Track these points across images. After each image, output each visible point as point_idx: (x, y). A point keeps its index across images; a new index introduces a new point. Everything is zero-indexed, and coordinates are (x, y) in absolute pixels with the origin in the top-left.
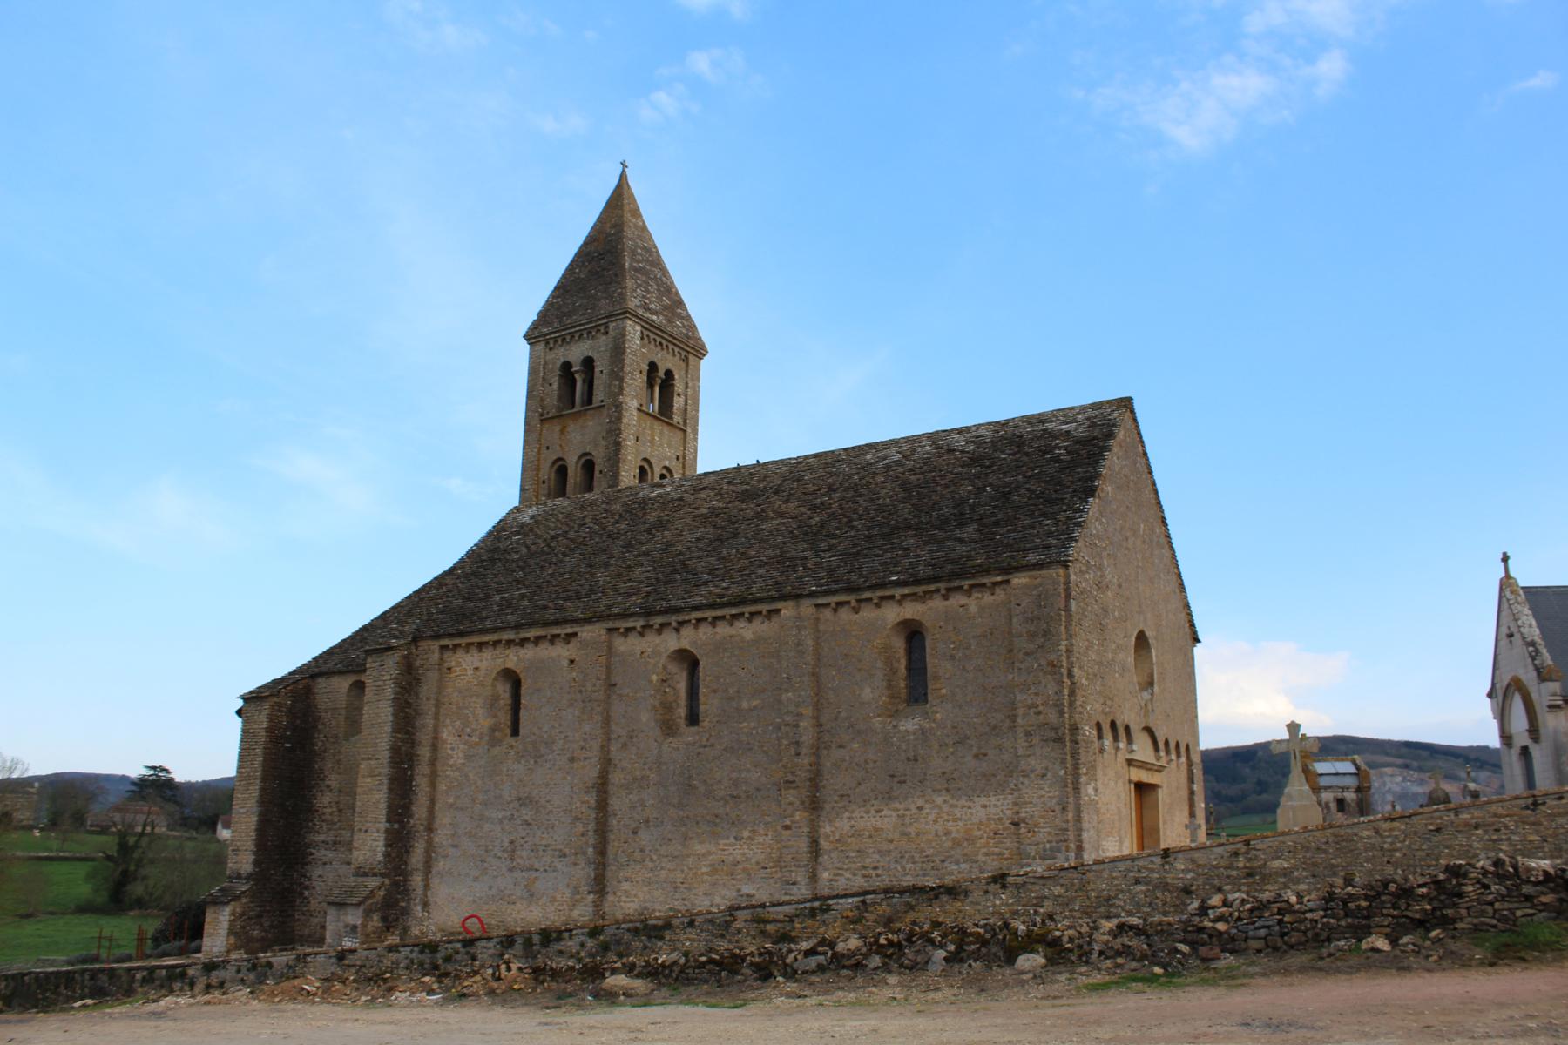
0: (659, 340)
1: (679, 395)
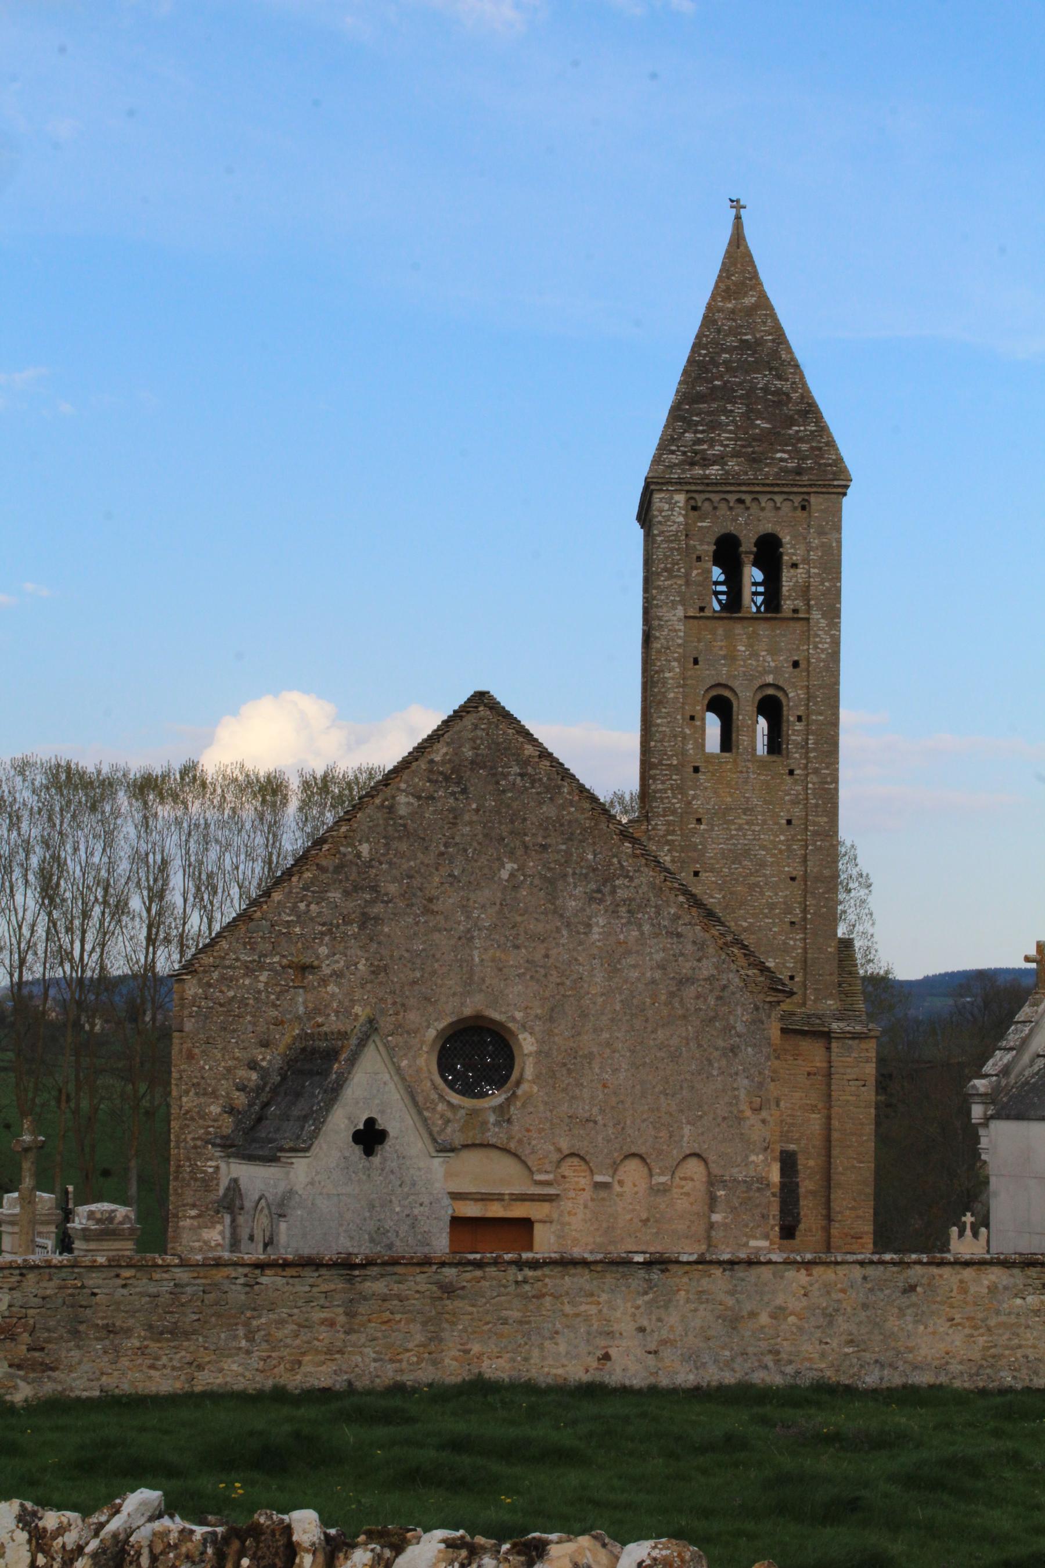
1: (795, 566)
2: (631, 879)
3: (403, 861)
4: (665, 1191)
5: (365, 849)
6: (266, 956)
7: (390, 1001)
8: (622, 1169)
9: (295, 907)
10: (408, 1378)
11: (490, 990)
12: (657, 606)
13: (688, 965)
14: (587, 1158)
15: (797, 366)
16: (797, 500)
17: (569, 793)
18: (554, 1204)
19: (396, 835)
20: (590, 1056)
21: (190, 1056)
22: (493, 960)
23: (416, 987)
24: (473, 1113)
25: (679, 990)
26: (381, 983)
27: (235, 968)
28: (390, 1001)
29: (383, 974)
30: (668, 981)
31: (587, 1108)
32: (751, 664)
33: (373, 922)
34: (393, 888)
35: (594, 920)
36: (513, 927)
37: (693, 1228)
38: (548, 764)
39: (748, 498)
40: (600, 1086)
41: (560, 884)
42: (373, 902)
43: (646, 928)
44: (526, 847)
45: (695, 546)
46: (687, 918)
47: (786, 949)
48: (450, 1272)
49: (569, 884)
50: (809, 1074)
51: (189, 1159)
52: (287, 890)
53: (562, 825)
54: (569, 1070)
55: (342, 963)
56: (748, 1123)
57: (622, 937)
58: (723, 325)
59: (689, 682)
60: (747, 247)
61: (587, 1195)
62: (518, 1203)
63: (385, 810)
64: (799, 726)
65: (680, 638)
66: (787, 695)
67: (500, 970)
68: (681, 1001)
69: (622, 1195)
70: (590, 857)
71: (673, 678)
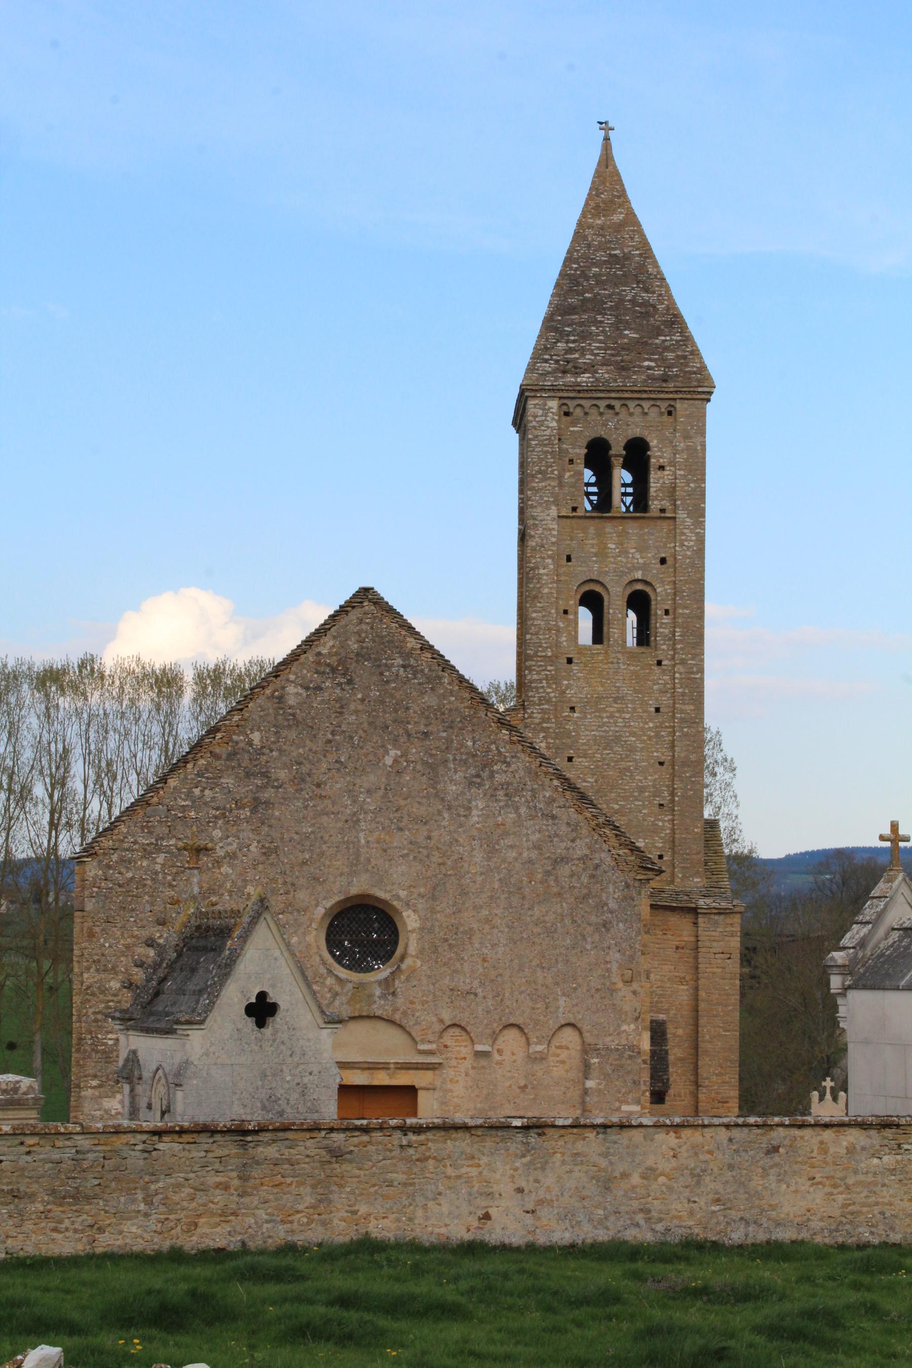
0: (602, 404)
1: (662, 468)
2: (508, 765)
3: (293, 748)
4: (542, 1059)
5: (256, 737)
6: (162, 839)
7: (280, 881)
8: (501, 1039)
9: (189, 794)
10: (299, 1239)
11: (375, 870)
12: (532, 507)
13: (563, 845)
14: (468, 1029)
15: (663, 279)
16: (664, 405)
17: (450, 684)
18: (437, 1072)
19: (286, 724)
20: (470, 933)
21: (91, 935)
22: (378, 842)
23: (305, 868)
24: (359, 987)
25: (554, 869)
26: (272, 864)
27: (133, 851)
28: (280, 881)
29: (274, 856)
30: (544, 861)
31: (468, 981)
32: (621, 561)
33: (264, 806)
34: (283, 774)
35: (474, 803)
36: (397, 811)
37: (569, 1094)
38: (429, 656)
39: (617, 404)
40: (480, 961)
41: (441, 770)
42: (264, 787)
43: (523, 810)
44: (409, 735)
45: (567, 449)
46: (562, 801)
47: (655, 830)
48: (338, 1137)
49: (450, 770)
50: (677, 948)
51: (90, 1032)
52: (182, 776)
53: (443, 714)
54: (450, 945)
55: (235, 845)
56: (620, 994)
57: (500, 819)
58: (593, 240)
59: (562, 578)
60: (615, 167)
61: (468, 1063)
62: (403, 1071)
63: (276, 700)
64: (666, 620)
65: (554, 536)
66: (655, 590)
67: (385, 851)
68: (556, 880)
69: (501, 1064)
70: (470, 743)
71: (547, 575)
